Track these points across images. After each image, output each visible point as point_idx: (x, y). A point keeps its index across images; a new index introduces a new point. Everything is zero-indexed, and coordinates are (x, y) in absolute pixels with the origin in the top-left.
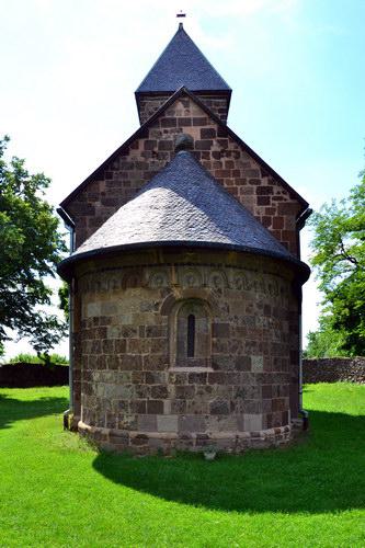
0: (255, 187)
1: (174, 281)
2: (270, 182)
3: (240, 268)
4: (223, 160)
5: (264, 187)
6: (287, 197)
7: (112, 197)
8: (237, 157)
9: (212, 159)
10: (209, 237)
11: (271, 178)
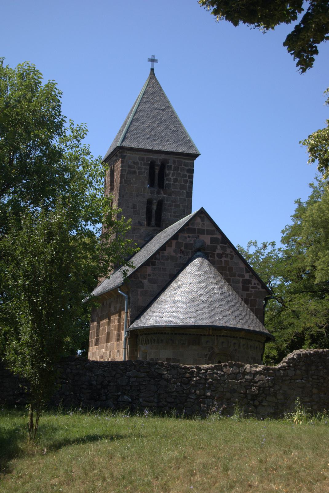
0: (241, 279)
2: (250, 276)
3: (246, 339)
4: (223, 259)
5: (246, 279)
6: (260, 287)
8: (232, 258)
9: (216, 258)
10: (233, 324)
11: (251, 274)
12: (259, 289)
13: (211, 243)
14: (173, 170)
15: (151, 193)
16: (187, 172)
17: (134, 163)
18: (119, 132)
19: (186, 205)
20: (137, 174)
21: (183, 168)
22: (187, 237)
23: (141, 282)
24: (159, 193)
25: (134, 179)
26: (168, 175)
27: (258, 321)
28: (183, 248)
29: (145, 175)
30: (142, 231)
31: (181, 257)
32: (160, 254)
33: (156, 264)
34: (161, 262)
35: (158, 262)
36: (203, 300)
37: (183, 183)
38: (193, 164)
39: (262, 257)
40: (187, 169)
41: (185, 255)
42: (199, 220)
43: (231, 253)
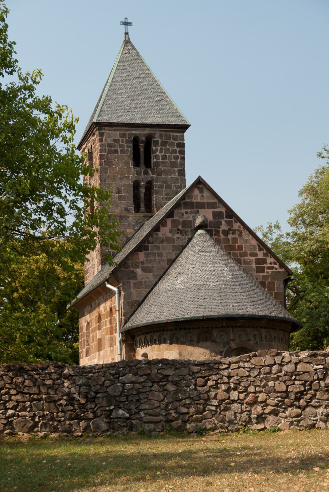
1: (232, 338)
2: (265, 255)
3: (268, 328)
4: (230, 236)
5: (260, 259)
6: (277, 266)
7: (150, 265)
8: (241, 234)
9: (222, 236)
10: (251, 310)
11: (265, 251)
12: (276, 269)
13: (213, 219)
14: (161, 146)
15: (137, 174)
16: (177, 147)
17: (114, 140)
18: (94, 111)
19: (180, 185)
20: (119, 154)
21: (172, 142)
22: (184, 213)
23: (133, 272)
24: (146, 173)
25: (116, 160)
26: (156, 151)
27: (280, 307)
28: (180, 227)
29: (129, 154)
30: (131, 218)
31: (178, 238)
32: (153, 237)
33: (150, 248)
34: (155, 246)
35: (151, 246)
36: (211, 285)
37: (173, 160)
38: (183, 138)
39: (271, 242)
40: (176, 143)
41: (183, 236)
42: (196, 192)
43: (239, 229)
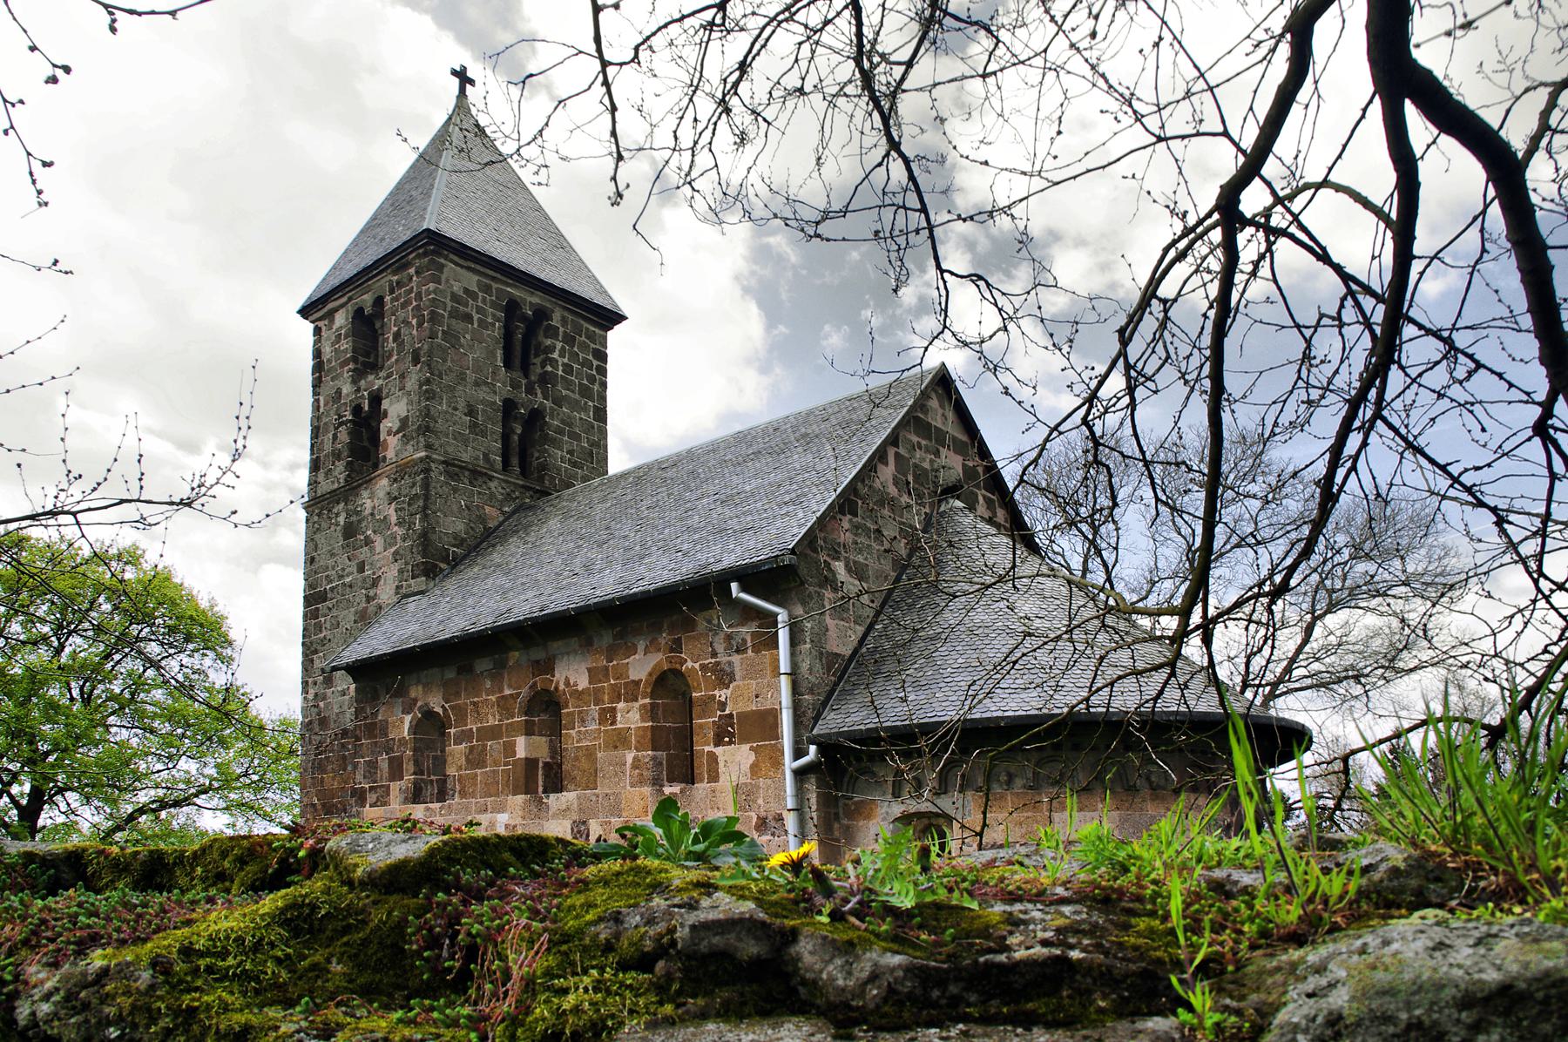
17: (466, 291)
37: (585, 382)
